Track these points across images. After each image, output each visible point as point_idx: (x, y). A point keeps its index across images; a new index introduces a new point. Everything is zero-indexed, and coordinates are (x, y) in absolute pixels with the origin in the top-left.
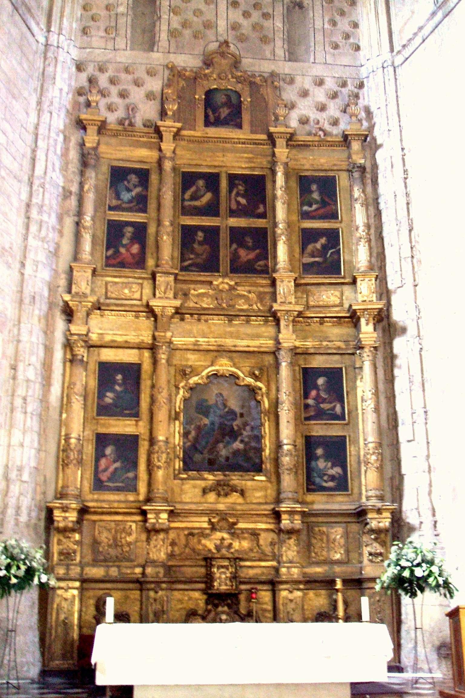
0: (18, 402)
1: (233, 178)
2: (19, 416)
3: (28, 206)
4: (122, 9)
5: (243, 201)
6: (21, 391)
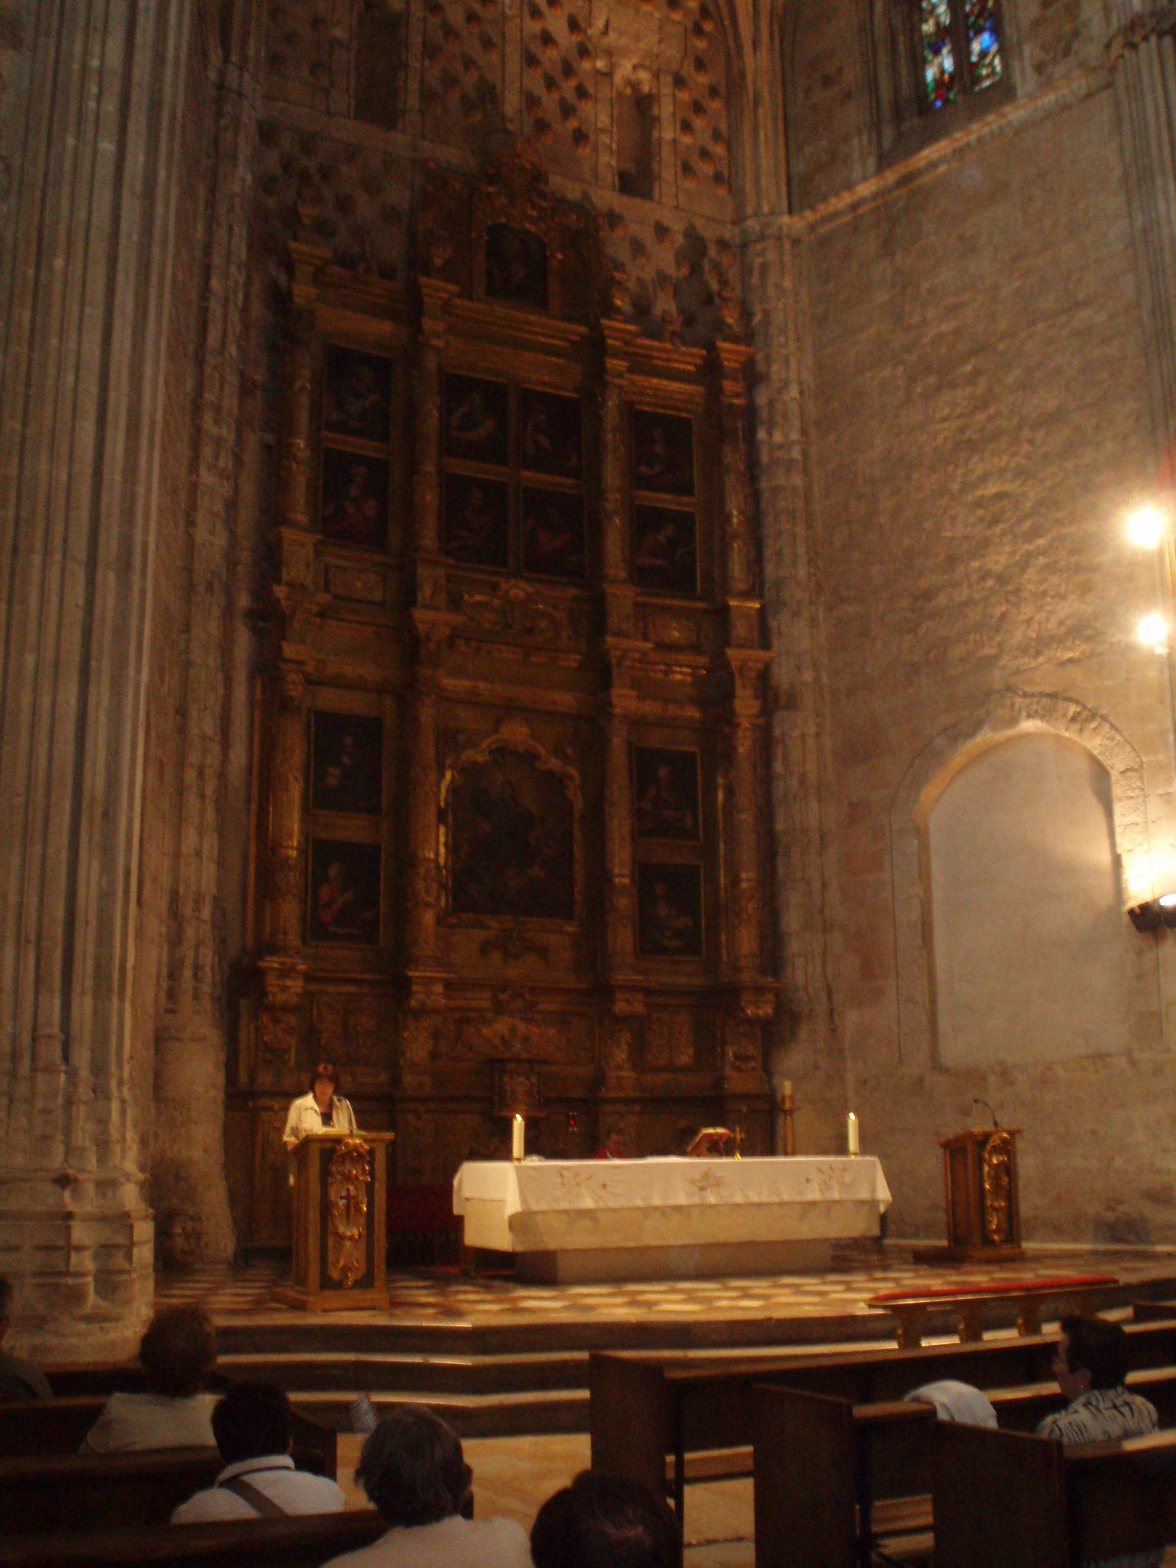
0: (191, 775)
2: (192, 801)
5: (544, 441)
6: (194, 757)
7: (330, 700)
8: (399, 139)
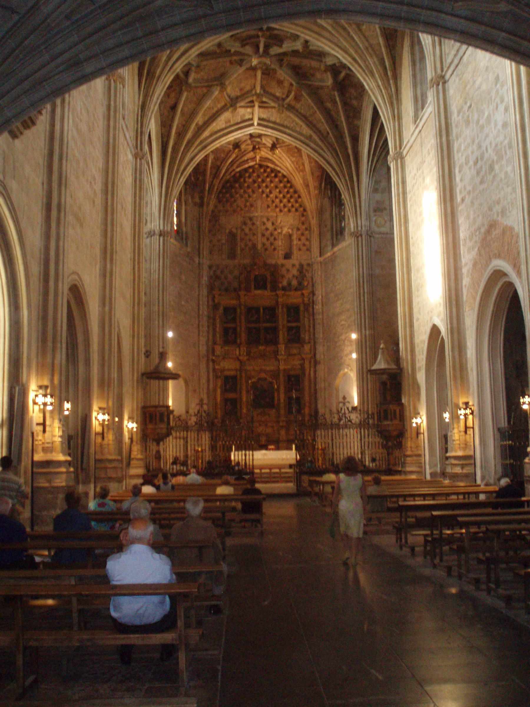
1: (265, 308)
3: (199, 325)
4: (223, 241)
7: (227, 373)
8: (236, 261)
